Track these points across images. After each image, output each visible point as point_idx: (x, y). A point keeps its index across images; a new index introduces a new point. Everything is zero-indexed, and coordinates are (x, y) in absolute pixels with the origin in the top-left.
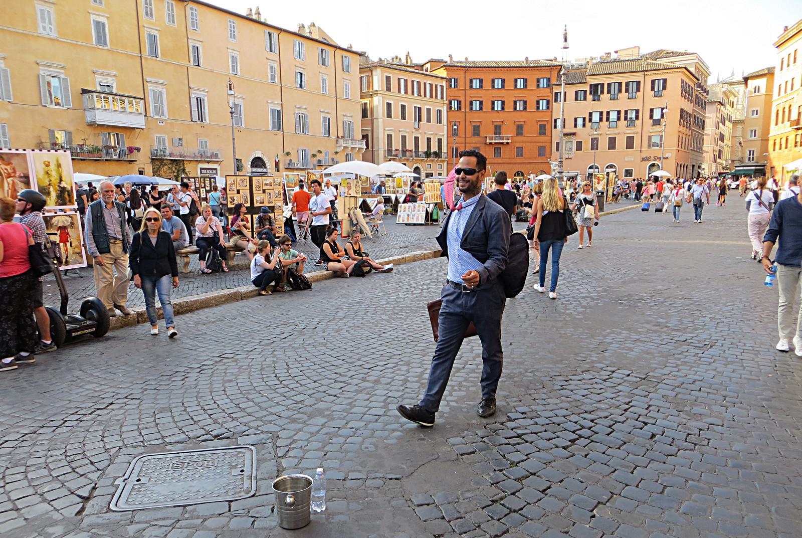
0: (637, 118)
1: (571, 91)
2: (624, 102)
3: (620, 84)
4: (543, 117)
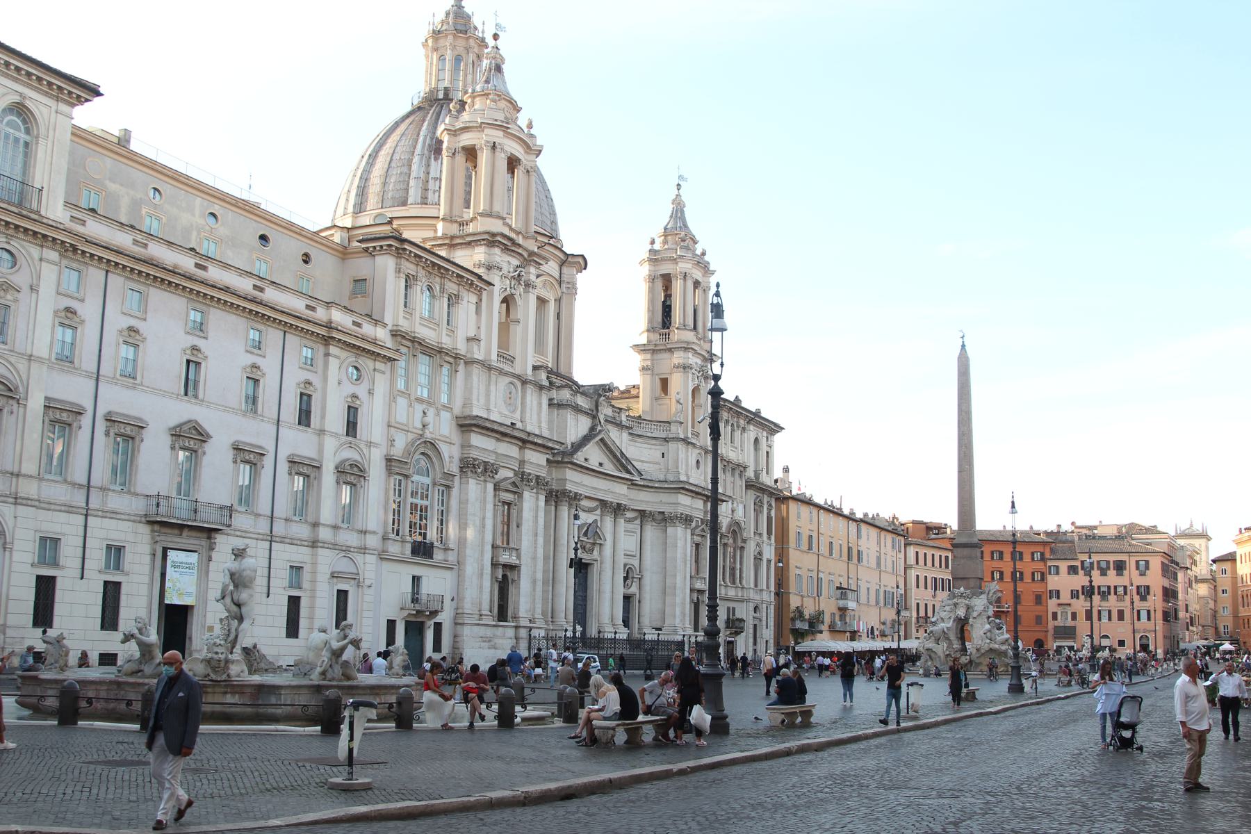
0: (1125, 593)
1: (1063, 566)
2: (1112, 579)
3: (1108, 562)
4: (1038, 588)
